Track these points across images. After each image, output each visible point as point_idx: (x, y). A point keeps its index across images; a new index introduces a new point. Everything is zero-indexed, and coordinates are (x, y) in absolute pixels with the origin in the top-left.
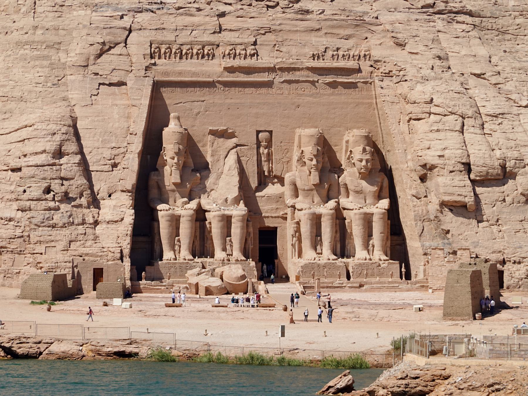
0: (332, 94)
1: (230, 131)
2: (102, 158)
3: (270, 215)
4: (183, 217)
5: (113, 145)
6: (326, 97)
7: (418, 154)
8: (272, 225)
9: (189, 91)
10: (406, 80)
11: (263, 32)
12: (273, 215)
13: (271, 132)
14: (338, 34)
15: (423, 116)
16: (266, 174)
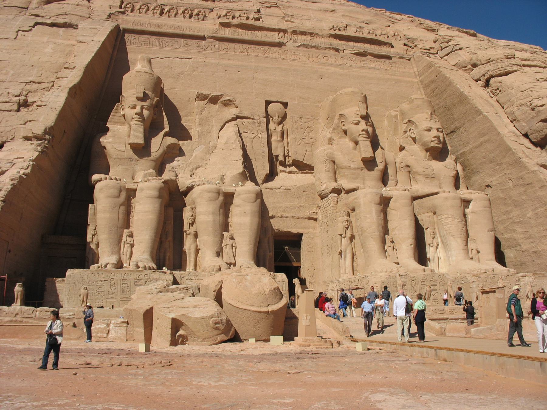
0: (363, 67)
1: (225, 98)
2: (6, 94)
3: (290, 215)
4: (142, 190)
5: (31, 79)
6: (356, 69)
7: (534, 105)
8: (294, 231)
9: (170, 46)
10: (460, 49)
11: (269, 6)
12: (297, 216)
13: (285, 105)
14: (358, 18)
15: (515, 68)
16: (281, 158)
